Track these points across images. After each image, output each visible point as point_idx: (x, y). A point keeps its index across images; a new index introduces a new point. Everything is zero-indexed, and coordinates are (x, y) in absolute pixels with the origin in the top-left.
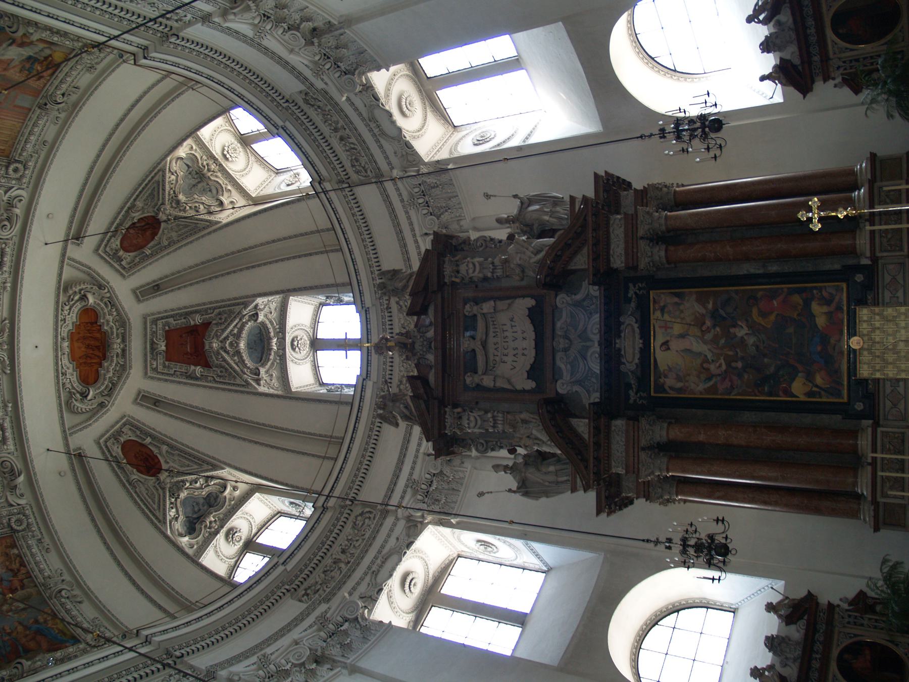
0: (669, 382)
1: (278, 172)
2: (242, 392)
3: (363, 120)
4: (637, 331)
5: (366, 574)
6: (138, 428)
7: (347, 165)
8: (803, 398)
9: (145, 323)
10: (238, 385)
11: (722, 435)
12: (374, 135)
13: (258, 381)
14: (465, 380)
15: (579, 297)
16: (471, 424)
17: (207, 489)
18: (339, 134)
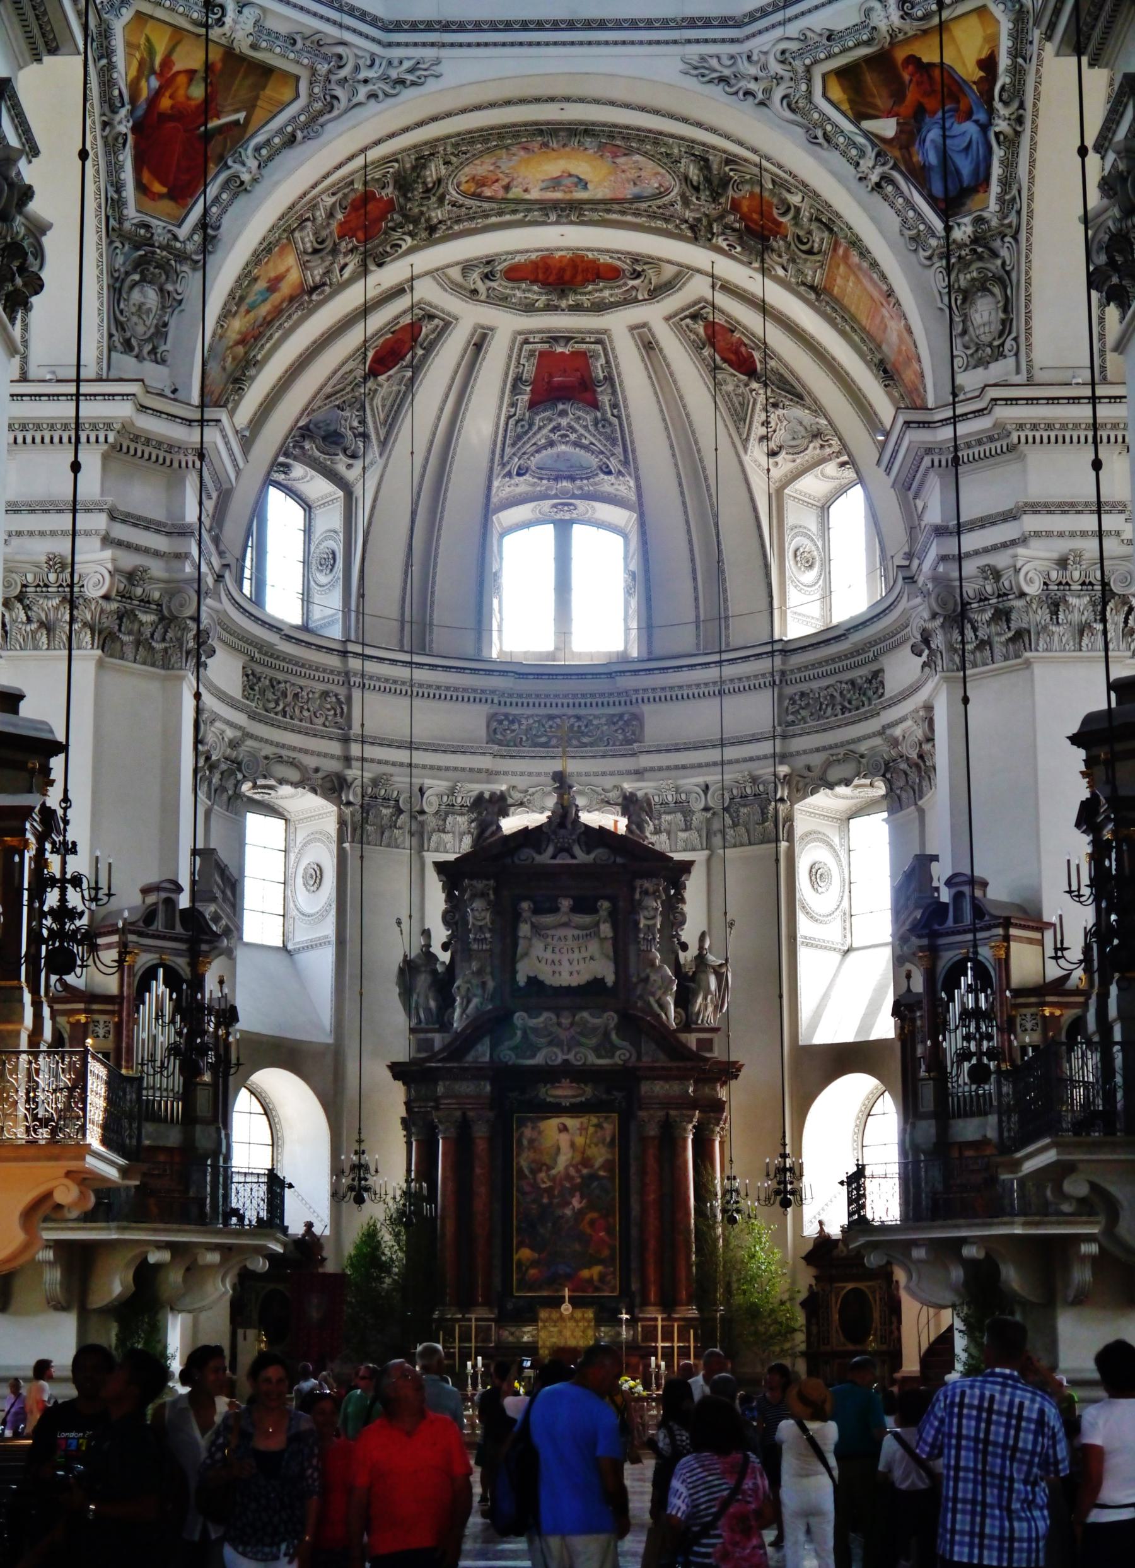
0: (528, 1132)
1: (824, 509)
2: (492, 460)
3: (849, 742)
4: (578, 1100)
5: (277, 745)
6: (440, 334)
7: (804, 687)
8: (515, 1257)
9: (598, 332)
10: (503, 450)
11: (482, 1190)
12: (831, 747)
13: (509, 474)
14: (525, 898)
15: (614, 1036)
16: (478, 913)
17: (349, 433)
18: (837, 695)
